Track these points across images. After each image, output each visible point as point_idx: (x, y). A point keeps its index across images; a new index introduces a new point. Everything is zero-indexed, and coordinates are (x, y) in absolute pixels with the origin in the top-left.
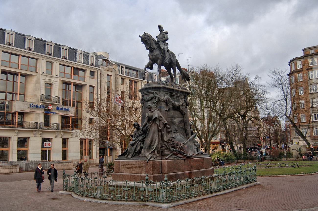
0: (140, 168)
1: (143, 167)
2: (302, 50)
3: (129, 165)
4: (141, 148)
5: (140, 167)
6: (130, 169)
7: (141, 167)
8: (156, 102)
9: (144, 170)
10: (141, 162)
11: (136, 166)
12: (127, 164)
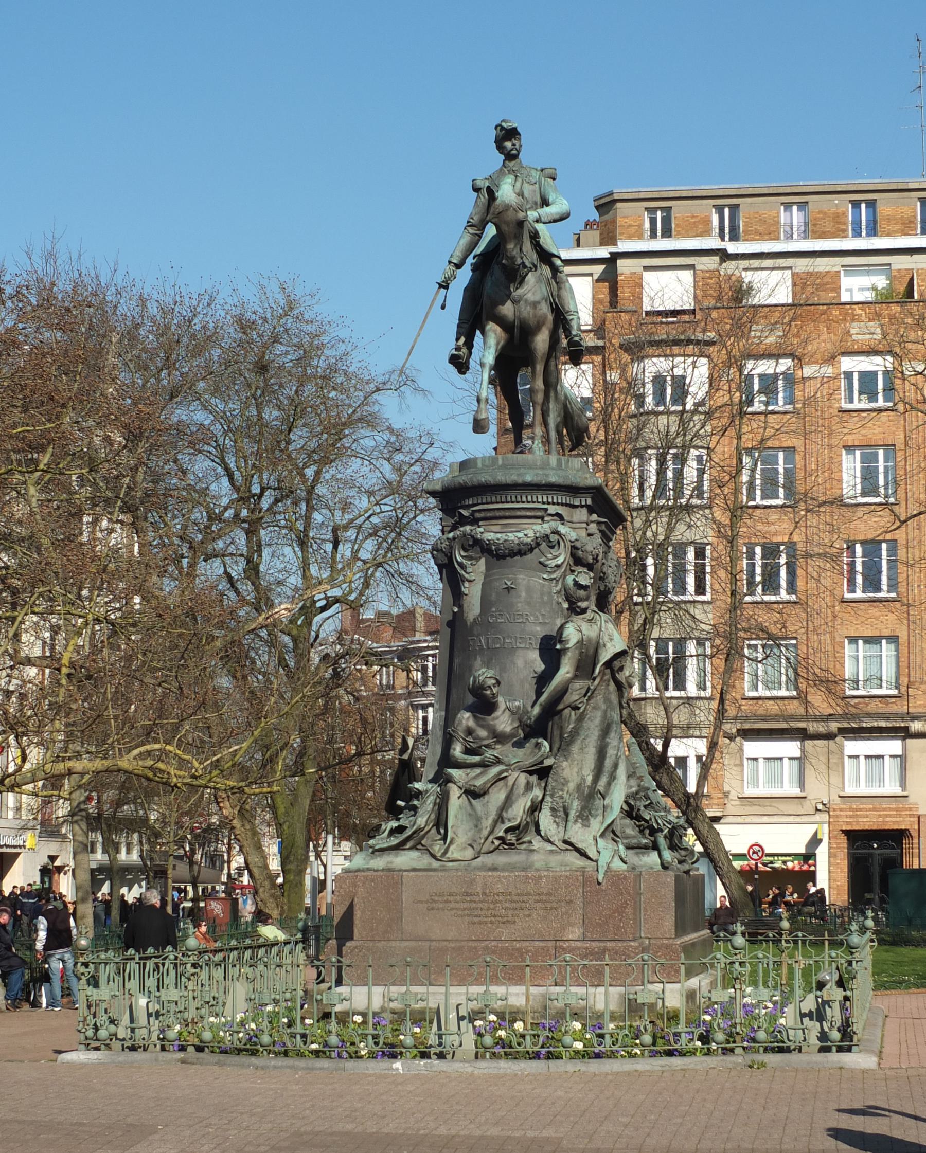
1: (570, 902)
2: (592, 204)
4: (535, 808)
5: (549, 906)
7: (555, 905)
8: (558, 566)
9: (577, 917)
11: (525, 898)
12: (454, 890)
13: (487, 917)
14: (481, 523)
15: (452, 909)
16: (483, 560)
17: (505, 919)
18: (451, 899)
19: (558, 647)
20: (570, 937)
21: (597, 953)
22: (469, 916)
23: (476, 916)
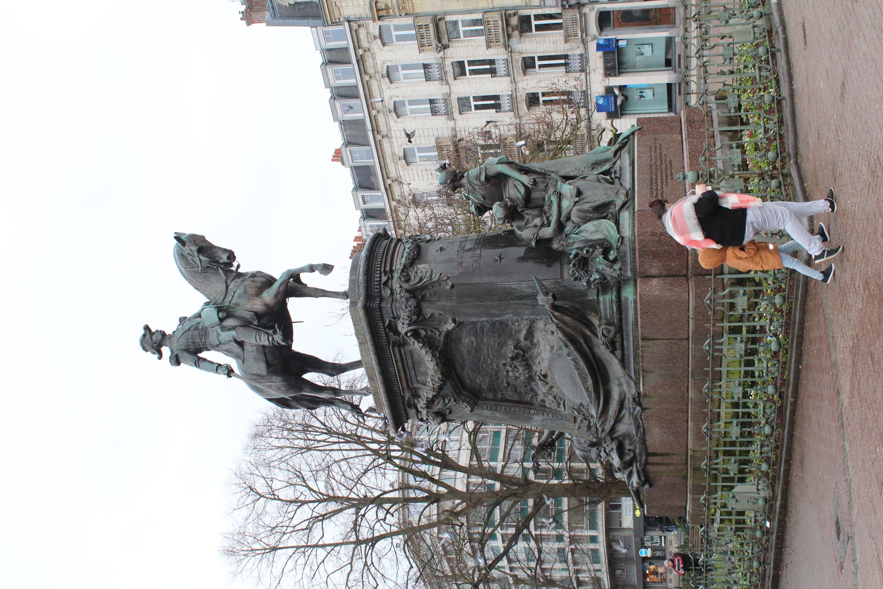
0: (660, 145)
3: (654, 181)
6: (669, 177)
7: (658, 145)
10: (638, 146)
13: (667, 173)
14: (394, 268)
15: (662, 187)
18: (654, 188)
19: (483, 178)
22: (667, 180)
23: (667, 176)
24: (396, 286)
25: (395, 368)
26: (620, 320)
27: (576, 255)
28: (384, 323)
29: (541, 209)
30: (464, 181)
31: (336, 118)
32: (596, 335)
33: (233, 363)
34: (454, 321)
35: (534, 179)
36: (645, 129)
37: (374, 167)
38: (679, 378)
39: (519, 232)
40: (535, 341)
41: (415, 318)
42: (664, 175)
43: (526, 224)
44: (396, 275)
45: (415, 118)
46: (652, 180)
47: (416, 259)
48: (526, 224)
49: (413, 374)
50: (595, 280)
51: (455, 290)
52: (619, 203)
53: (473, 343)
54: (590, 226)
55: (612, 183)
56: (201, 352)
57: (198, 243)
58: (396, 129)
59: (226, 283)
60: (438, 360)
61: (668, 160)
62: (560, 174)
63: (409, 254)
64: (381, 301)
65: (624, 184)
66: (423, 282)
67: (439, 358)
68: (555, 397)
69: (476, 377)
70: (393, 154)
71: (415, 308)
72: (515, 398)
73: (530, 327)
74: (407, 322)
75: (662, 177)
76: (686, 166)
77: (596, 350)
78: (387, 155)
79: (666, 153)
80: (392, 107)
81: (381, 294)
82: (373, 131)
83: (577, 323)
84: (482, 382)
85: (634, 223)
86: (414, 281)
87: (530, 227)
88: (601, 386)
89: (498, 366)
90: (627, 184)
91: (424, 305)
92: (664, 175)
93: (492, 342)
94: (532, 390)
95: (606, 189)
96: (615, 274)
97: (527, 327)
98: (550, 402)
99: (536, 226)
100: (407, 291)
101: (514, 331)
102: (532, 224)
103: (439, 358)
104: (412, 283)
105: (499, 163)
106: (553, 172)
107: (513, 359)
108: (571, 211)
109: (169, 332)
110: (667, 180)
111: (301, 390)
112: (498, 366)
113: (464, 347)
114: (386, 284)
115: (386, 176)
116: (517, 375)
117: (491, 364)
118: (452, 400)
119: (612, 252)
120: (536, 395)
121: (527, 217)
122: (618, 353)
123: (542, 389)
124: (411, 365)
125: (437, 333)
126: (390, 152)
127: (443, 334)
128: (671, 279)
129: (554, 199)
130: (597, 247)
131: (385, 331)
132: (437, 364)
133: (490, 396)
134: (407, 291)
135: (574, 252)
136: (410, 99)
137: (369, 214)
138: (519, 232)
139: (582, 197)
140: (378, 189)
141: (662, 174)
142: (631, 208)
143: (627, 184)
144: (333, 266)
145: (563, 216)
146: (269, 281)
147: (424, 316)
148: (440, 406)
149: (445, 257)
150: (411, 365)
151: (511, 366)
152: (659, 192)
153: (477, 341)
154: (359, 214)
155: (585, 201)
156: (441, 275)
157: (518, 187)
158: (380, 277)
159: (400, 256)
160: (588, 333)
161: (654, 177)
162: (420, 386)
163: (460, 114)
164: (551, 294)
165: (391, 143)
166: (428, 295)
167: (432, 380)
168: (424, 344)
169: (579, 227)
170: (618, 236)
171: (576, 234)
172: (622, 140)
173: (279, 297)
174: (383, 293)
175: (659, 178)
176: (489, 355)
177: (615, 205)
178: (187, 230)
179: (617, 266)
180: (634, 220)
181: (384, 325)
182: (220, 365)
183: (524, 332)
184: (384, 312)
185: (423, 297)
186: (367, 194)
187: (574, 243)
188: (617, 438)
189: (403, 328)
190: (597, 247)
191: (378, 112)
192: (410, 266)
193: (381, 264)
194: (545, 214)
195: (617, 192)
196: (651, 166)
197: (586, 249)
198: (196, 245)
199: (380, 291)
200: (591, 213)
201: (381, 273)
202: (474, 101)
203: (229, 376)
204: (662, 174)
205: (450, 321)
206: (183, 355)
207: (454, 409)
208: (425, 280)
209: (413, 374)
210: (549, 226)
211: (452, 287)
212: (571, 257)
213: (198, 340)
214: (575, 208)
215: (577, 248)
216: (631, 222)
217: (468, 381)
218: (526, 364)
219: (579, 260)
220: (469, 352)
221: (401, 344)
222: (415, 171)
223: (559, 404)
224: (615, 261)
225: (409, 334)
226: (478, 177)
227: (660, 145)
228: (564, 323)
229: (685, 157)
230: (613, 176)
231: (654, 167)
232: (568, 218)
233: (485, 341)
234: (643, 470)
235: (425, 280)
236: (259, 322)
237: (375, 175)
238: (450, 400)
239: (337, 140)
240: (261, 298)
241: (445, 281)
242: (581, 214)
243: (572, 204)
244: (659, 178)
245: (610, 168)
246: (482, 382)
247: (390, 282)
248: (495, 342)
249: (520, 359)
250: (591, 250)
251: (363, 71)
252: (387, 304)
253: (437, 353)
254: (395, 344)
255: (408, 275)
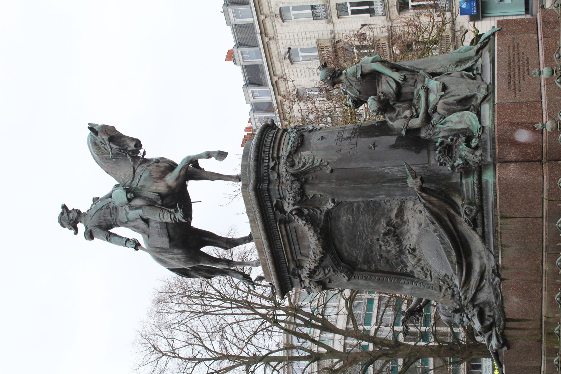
0: (518, 44)
3: (512, 76)
6: (526, 72)
7: (516, 44)
10: (498, 45)
13: (524, 69)
14: (280, 155)
16: (302, 153)
17: (525, 61)
18: (512, 82)
19: (359, 75)
20: (536, 38)
21: (545, 23)
22: (523, 76)
23: (524, 72)
24: (282, 170)
25: (282, 242)
26: (481, 200)
27: (442, 143)
28: (272, 203)
29: (410, 102)
30: (342, 78)
31: (228, 23)
32: (459, 214)
33: (140, 238)
34: (333, 201)
35: (404, 76)
36: (504, 29)
37: (262, 66)
38: (534, 252)
39: (391, 123)
40: (405, 218)
41: (299, 198)
42: (521, 71)
43: (397, 116)
44: (282, 161)
45: (298, 22)
46: (510, 75)
47: (300, 147)
48: (397, 116)
49: (297, 247)
50: (459, 165)
51: (334, 175)
52: (480, 96)
53: (349, 220)
54: (454, 117)
55: (474, 79)
56: (111, 228)
57: (108, 132)
58: (281, 32)
59: (134, 168)
60: (319, 236)
61: (525, 58)
62: (428, 71)
63: (294, 142)
64: (269, 184)
65: (485, 79)
66: (306, 167)
67: (320, 233)
68: (422, 269)
69: (352, 251)
70: (279, 54)
71: (299, 189)
72: (387, 269)
73: (401, 206)
74: (292, 202)
75: (519, 73)
76: (541, 63)
77: (459, 227)
78: (274, 55)
79: (523, 51)
80: (278, 12)
81: (269, 178)
82: (261, 33)
83: (442, 203)
84: (358, 255)
85: (493, 114)
86: (298, 165)
87: (400, 118)
88: (464, 259)
89: (372, 241)
90: (488, 79)
91: (307, 187)
92: (521, 71)
93: (367, 220)
94: (402, 262)
95: (469, 84)
96: (476, 160)
97: (398, 206)
98: (418, 273)
99: (406, 117)
100: (292, 175)
101: (386, 210)
102: (403, 116)
103: (320, 233)
104: (296, 168)
105: (373, 61)
106: (421, 69)
107: (385, 234)
108: (437, 103)
109: (83, 210)
110: (523, 76)
111: (199, 261)
112: (372, 241)
113: (342, 224)
114: (273, 168)
115: (273, 73)
116: (389, 248)
117: (366, 239)
118: (332, 270)
119: (473, 141)
120: (406, 266)
121: (398, 109)
122: (479, 229)
123: (411, 261)
124: (295, 240)
125: (318, 211)
126: (276, 53)
127: (324, 213)
128: (527, 164)
129: (422, 93)
130: (461, 135)
131: (273, 210)
132: (318, 239)
133: (365, 267)
134: (292, 175)
135: (439, 140)
136: (294, 5)
137: (257, 108)
138: (391, 123)
139: (447, 91)
140: (266, 85)
141: (519, 70)
142: (491, 100)
143: (488, 79)
144: (227, 153)
145: (430, 108)
146: (172, 166)
147: (306, 196)
148: (320, 276)
149: (326, 145)
150: (295, 240)
151: (384, 241)
152: (517, 86)
153: (354, 219)
154: (249, 107)
155: (450, 95)
156: (321, 161)
157: (390, 83)
158: (269, 162)
159: (286, 144)
160: (452, 212)
161: (512, 73)
162: (303, 258)
163: (338, 18)
164: (419, 177)
165: (277, 44)
166: (311, 178)
167: (314, 253)
168: (307, 222)
169: (445, 118)
170: (480, 126)
171: (442, 124)
172: (484, 40)
173: (180, 179)
174: (271, 176)
175: (517, 74)
176: (364, 230)
177: (477, 98)
178: (100, 121)
179: (478, 153)
180: (494, 111)
181: (272, 205)
182: (128, 239)
183: (395, 211)
184: (272, 193)
185: (306, 181)
186: (257, 89)
187: (440, 132)
188: (478, 305)
189: (288, 207)
190: (461, 135)
191: (266, 17)
192: (295, 153)
193: (269, 151)
194: (414, 107)
195: (479, 87)
196: (509, 63)
197: (451, 137)
198: (107, 134)
199: (269, 175)
200: (455, 106)
201: (269, 160)
202: (351, 6)
203: (136, 249)
204: (519, 70)
205: (330, 201)
206: (96, 231)
207: (333, 278)
208: (308, 165)
209: (297, 247)
210: (418, 117)
211: (332, 171)
212: (437, 144)
213: (109, 218)
214: (441, 101)
215: (442, 137)
216: (491, 113)
217: (346, 254)
218: (397, 240)
219: (445, 148)
220: (346, 228)
221: (286, 222)
222: (298, 69)
223: (426, 274)
224: (476, 148)
225: (294, 213)
226: (354, 75)
227: (518, 44)
228: (430, 203)
229: (541, 54)
230: (475, 72)
231: (512, 64)
232: (435, 110)
233: (360, 218)
234: (502, 334)
235: (308, 165)
236: (162, 202)
237: (263, 73)
238: (329, 271)
239: (230, 43)
240: (164, 181)
241: (326, 166)
242: (446, 106)
243: (439, 97)
244: (517, 74)
245: (472, 66)
246: (358, 255)
247: (277, 167)
248: (369, 220)
249: (391, 235)
250: (455, 139)
251: (259, 11)
252: (274, 186)
253: (318, 229)
254: (281, 221)
255: (293, 160)
